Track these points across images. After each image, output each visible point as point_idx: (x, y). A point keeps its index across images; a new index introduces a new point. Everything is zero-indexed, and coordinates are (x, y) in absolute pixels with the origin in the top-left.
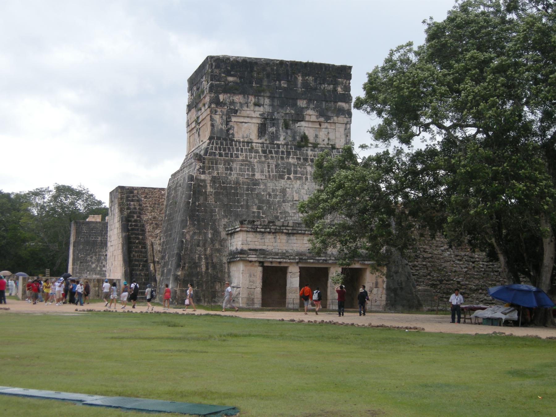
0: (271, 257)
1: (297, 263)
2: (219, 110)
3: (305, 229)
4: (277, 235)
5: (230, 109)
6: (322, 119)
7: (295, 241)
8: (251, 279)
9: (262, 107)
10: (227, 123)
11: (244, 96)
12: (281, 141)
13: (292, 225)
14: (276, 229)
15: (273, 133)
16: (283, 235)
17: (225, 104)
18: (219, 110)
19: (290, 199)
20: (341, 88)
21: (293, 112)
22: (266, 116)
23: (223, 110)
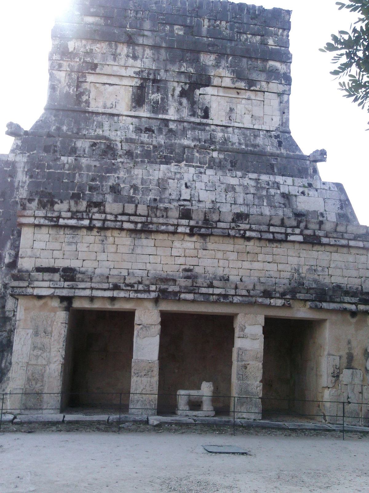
0: (88, 285)
2: (65, 64)
3: (175, 222)
4: (109, 233)
5: (85, 62)
6: (242, 85)
7: (152, 250)
8: (38, 340)
9: (139, 61)
10: (79, 84)
11: (110, 45)
12: (172, 114)
13: (146, 213)
14: (105, 220)
15: (157, 102)
16: (124, 233)
18: (65, 64)
19: (173, 197)
20: (274, 41)
21: (192, 71)
22: (145, 75)
23: (72, 64)
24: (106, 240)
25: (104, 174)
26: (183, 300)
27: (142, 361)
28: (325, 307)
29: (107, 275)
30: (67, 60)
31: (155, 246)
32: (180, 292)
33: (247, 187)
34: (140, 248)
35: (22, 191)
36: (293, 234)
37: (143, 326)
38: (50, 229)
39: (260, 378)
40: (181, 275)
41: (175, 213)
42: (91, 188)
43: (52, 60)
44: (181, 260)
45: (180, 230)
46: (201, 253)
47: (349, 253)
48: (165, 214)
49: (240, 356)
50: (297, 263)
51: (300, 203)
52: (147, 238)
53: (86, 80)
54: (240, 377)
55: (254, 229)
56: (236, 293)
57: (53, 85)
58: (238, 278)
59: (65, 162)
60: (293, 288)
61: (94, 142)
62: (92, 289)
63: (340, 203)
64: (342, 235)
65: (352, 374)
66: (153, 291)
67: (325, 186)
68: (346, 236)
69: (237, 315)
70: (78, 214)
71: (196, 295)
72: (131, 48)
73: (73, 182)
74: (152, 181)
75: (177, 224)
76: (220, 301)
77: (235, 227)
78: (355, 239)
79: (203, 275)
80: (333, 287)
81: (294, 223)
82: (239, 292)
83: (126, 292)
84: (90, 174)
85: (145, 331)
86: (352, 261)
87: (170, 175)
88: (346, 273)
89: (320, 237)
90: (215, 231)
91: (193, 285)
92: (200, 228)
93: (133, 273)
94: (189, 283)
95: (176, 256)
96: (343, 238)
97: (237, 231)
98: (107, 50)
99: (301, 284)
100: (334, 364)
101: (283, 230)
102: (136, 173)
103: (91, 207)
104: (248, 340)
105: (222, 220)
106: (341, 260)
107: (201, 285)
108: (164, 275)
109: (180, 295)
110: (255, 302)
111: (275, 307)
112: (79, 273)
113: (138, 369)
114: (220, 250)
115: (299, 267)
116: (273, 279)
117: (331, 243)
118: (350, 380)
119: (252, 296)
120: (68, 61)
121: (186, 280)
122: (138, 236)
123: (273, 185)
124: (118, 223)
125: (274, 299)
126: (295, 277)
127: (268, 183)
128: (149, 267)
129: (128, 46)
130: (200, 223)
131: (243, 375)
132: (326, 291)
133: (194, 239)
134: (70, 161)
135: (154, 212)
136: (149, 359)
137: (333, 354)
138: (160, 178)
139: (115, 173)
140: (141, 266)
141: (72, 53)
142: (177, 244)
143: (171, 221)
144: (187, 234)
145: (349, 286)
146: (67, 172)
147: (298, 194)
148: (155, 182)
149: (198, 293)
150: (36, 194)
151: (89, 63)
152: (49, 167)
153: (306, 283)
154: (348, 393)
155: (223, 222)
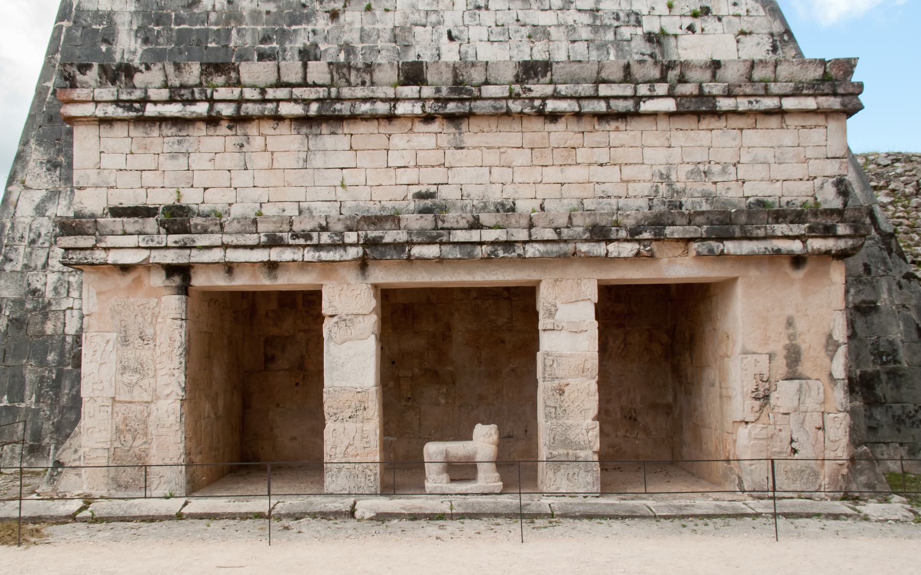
0: (216, 239)
4: (252, 129)
7: (346, 159)
13: (326, 79)
14: (240, 101)
16: (284, 128)
24: (248, 143)
25: (285, 27)
26: (418, 259)
27: (344, 389)
28: (732, 251)
29: (253, 216)
32: (411, 243)
33: (574, 29)
34: (319, 155)
36: (651, 97)
37: (340, 318)
38: (132, 127)
39: (594, 410)
40: (412, 206)
41: (387, 74)
45: (402, 109)
46: (453, 156)
47: (782, 128)
48: (367, 78)
49: (548, 369)
50: (664, 161)
51: (686, 49)
52: (333, 133)
54: (550, 413)
55: (563, 93)
56: (530, 236)
58: (536, 204)
60: (656, 216)
62: (225, 246)
63: (771, 40)
64: (766, 88)
65: (800, 390)
66: (351, 245)
67: (736, 8)
68: (774, 88)
69: (539, 282)
70: (183, 92)
71: (444, 248)
73: (226, 46)
74: (381, 33)
75: (393, 96)
76: (497, 256)
77: (521, 92)
78: (796, 93)
79: (459, 203)
80: (749, 206)
82: (538, 233)
83: (296, 250)
84: (259, 28)
85: (344, 327)
86: (790, 144)
87: (415, 17)
88: (779, 172)
89: (714, 97)
90: (480, 106)
91: (436, 226)
92: (447, 100)
93: (309, 209)
94: (427, 221)
95: (399, 167)
96: (767, 94)
97: (527, 101)
99: (676, 207)
100: (757, 372)
101: (628, 90)
102: (348, 19)
103: (211, 74)
104: (564, 334)
105: (493, 80)
106: (765, 144)
107: (455, 225)
108: (375, 210)
109: (409, 251)
110: (574, 254)
112: (199, 215)
113: (335, 406)
114: (491, 148)
115: (669, 170)
116: (613, 201)
117: (741, 109)
118: (796, 403)
119: (566, 241)
121: (422, 217)
122: (315, 130)
123: (627, 19)
124: (270, 106)
125: (616, 244)
126: (660, 191)
127: (618, 15)
128: (341, 194)
130: (444, 92)
131: (556, 408)
132: (733, 217)
133: (435, 127)
135: (344, 75)
136: (357, 386)
137: (755, 350)
138: (397, 25)
139: (308, 22)
140: (325, 194)
143: (380, 92)
144: (417, 117)
145: (784, 200)
146: (215, 28)
147: (679, 32)
148: (387, 35)
149: (449, 243)
152: (179, 20)
153: (688, 204)
154: (791, 431)
155: (496, 84)
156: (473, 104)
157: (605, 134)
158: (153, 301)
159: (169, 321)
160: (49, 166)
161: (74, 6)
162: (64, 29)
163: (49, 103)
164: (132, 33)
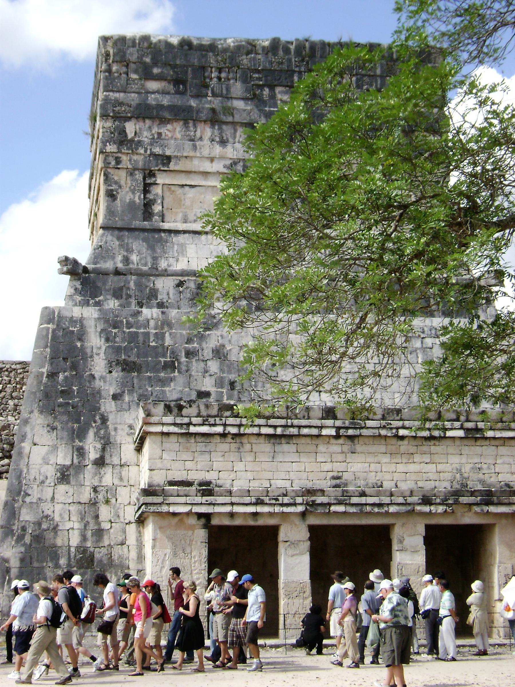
0: (227, 500)
1: (303, 515)
3: (318, 423)
4: (245, 440)
5: (152, 154)
7: (294, 457)
9: (229, 147)
10: (146, 189)
14: (240, 426)
16: (262, 439)
17: (139, 143)
18: (124, 158)
23: (135, 157)
24: (243, 447)
26: (334, 512)
30: (127, 151)
31: (297, 452)
35: (97, 361)
36: (451, 429)
38: (180, 437)
40: (329, 483)
42: (189, 354)
43: (106, 152)
44: (327, 467)
53: (156, 180)
57: (112, 190)
58: (393, 484)
59: (149, 317)
61: (180, 281)
62: (232, 504)
66: (299, 504)
69: (393, 525)
72: (217, 127)
73: (163, 345)
81: (454, 416)
90: (364, 432)
92: (347, 428)
98: (183, 133)
111: (436, 514)
115: (461, 466)
120: (128, 153)
128: (292, 476)
129: (213, 126)
133: (341, 441)
134: (155, 316)
140: (283, 475)
141: (132, 140)
142: (322, 448)
150: (116, 365)
151: (159, 155)
152: (129, 325)
153: (470, 484)
156: (361, 431)
157: (428, 447)
158: (190, 533)
159: (199, 543)
160: (48, 428)
161: (56, 314)
162: (51, 330)
163: (45, 384)
164: (98, 334)
